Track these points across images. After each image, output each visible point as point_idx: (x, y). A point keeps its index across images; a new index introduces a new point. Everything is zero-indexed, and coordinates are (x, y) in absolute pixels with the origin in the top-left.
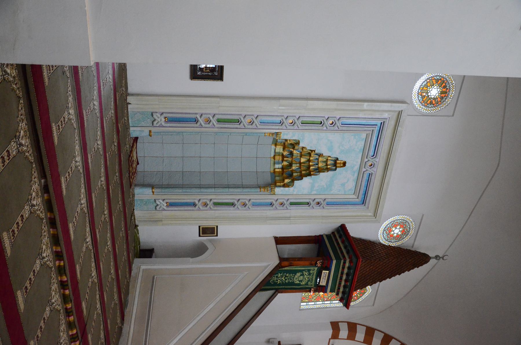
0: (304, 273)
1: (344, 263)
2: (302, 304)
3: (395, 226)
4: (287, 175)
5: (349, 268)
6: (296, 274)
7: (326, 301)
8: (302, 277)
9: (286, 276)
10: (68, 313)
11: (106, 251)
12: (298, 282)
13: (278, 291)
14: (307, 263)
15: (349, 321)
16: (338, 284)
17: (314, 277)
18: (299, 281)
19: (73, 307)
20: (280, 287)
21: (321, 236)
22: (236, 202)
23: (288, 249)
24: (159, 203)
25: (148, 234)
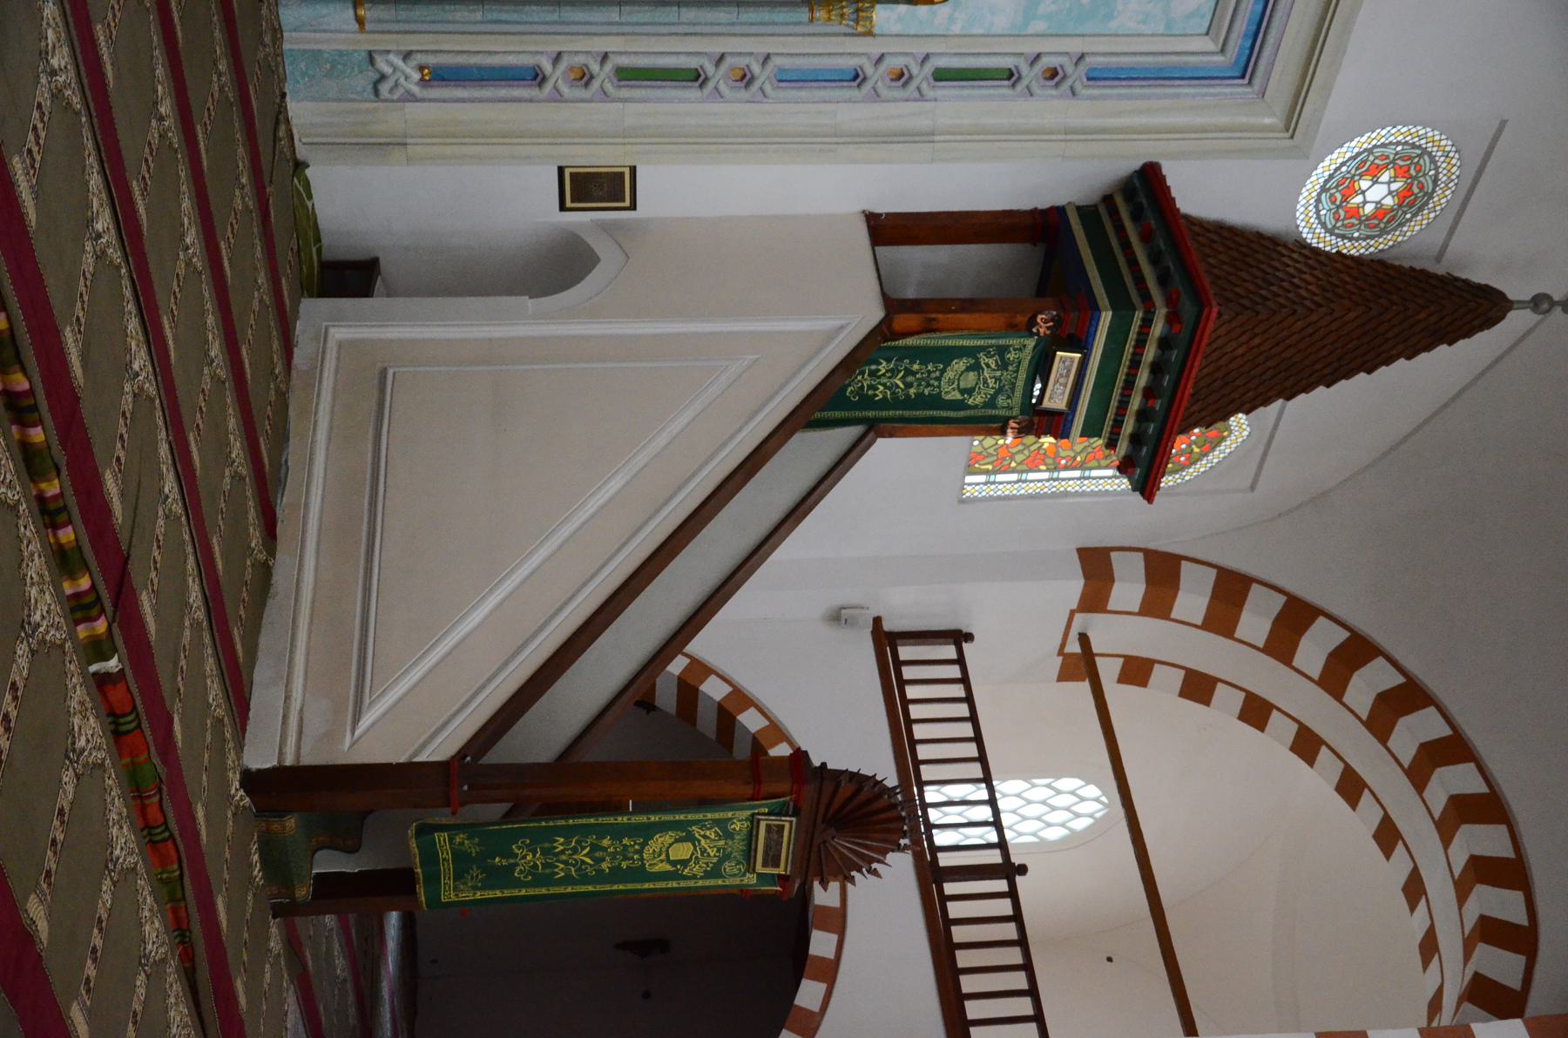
1: (1147, 323)
2: (969, 479)
3: (1374, 173)
5: (1164, 343)
6: (947, 364)
7: (1066, 468)
8: (972, 375)
9: (909, 372)
10: (49, 514)
11: (181, 268)
13: (876, 428)
14: (998, 320)
15: (1152, 546)
16: (1114, 404)
17: (1022, 375)
18: (963, 392)
19: (69, 491)
20: (884, 414)
21: (1058, 212)
22: (710, 68)
23: (923, 265)
24: (387, 70)
25: (351, 198)
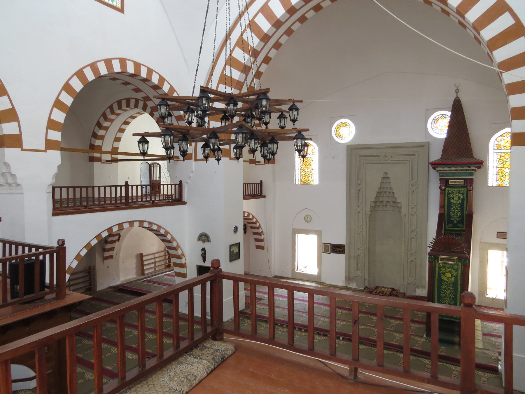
1: (440, 170)
9: (454, 209)
12: (460, 201)
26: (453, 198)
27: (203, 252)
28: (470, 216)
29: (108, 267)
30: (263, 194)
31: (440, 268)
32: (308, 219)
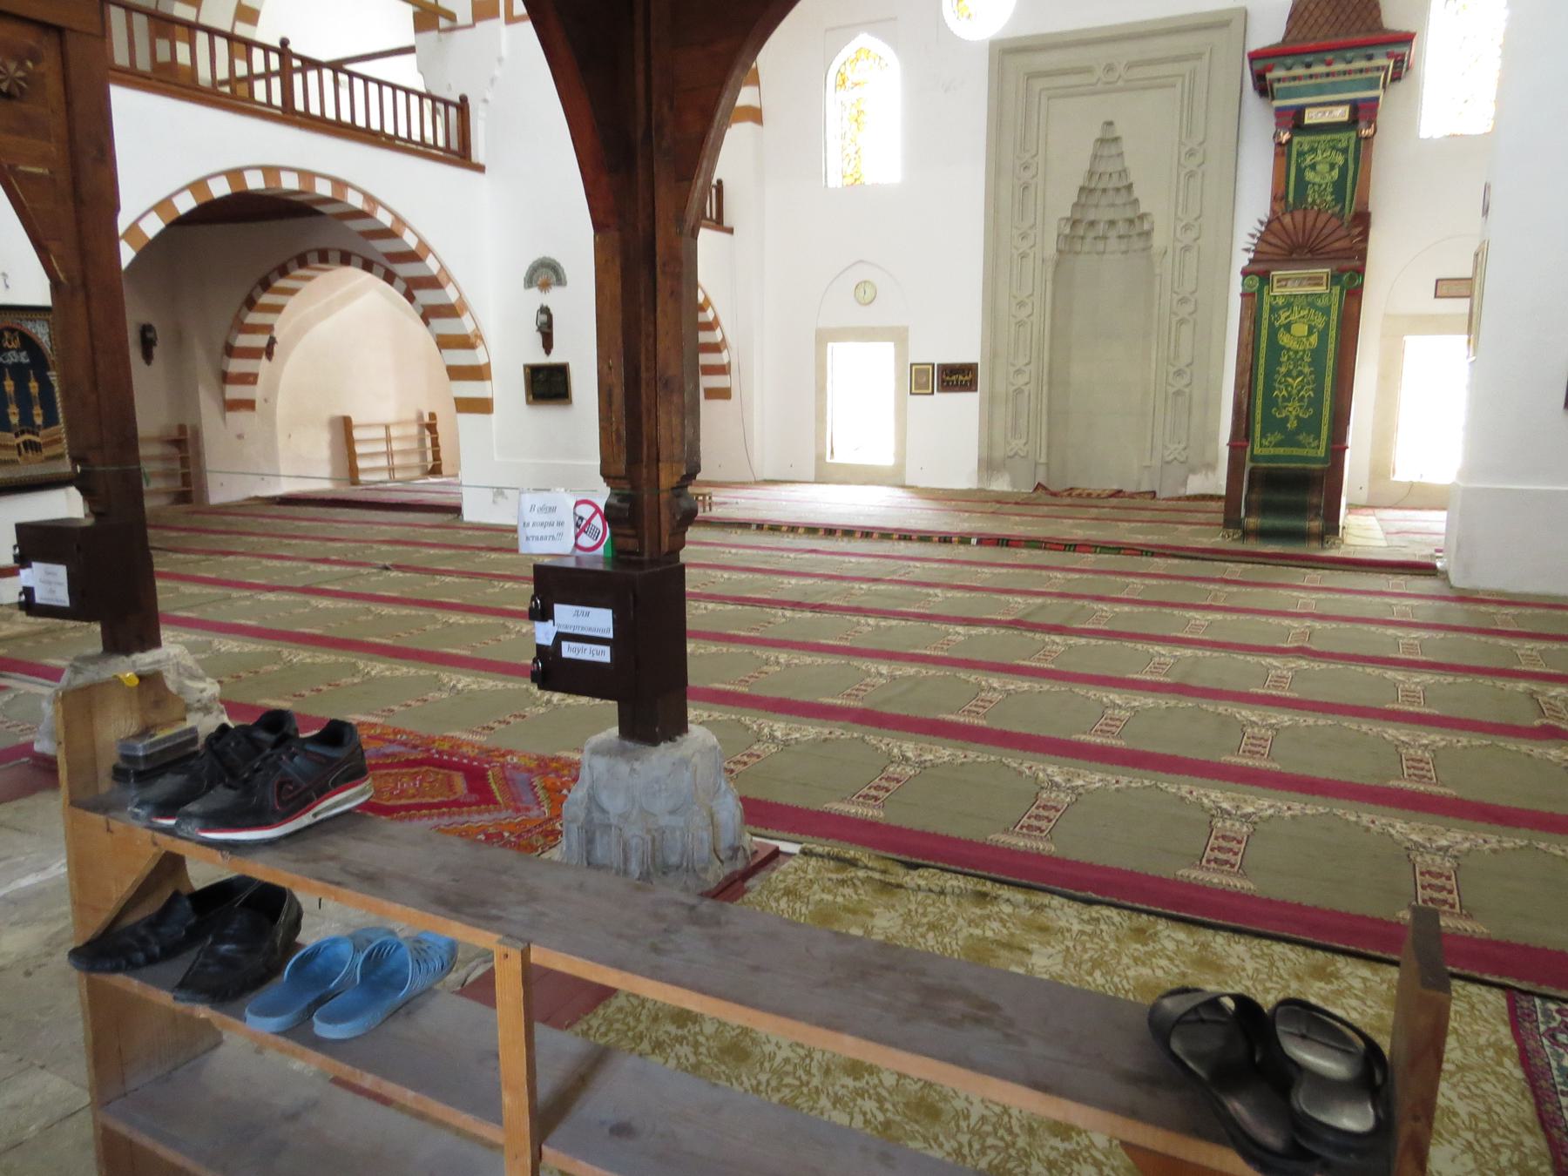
0: (1308, 162)
1: (1279, 80)
4: (1137, 227)
8: (1318, 167)
12: (1335, 174)
17: (1323, 137)
26: (1313, 167)
27: (544, 318)
28: (1363, 220)
29: (240, 437)
30: (726, 223)
31: (1274, 310)
32: (865, 294)
